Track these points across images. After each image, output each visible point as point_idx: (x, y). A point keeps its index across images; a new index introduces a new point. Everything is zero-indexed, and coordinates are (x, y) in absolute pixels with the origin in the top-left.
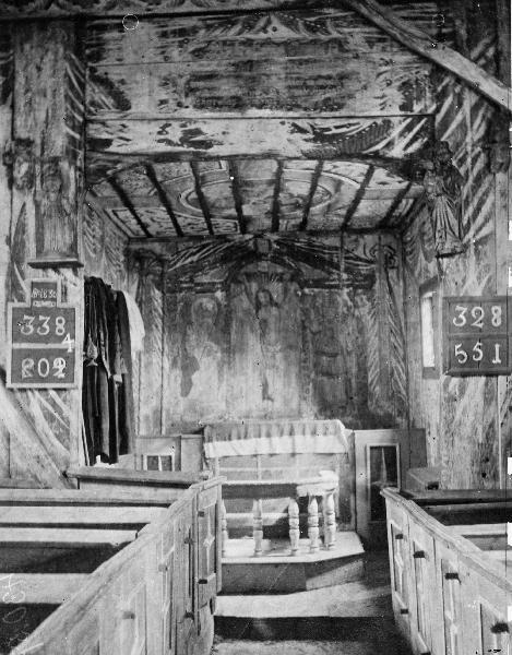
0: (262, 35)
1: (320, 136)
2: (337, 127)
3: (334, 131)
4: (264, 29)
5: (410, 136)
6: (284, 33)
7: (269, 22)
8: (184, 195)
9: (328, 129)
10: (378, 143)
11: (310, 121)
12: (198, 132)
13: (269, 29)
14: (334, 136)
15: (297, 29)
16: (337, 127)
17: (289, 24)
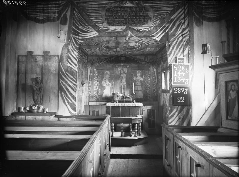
0: (125, 5)
1: (139, 31)
2: (143, 29)
3: (143, 30)
4: (125, 4)
5: (162, 31)
6: (130, 5)
7: (126, 2)
8: (103, 45)
9: (141, 29)
10: (154, 33)
11: (136, 27)
12: (108, 30)
13: (127, 3)
14: (143, 31)
15: (133, 4)
16: (143, 29)
17: (131, 3)
